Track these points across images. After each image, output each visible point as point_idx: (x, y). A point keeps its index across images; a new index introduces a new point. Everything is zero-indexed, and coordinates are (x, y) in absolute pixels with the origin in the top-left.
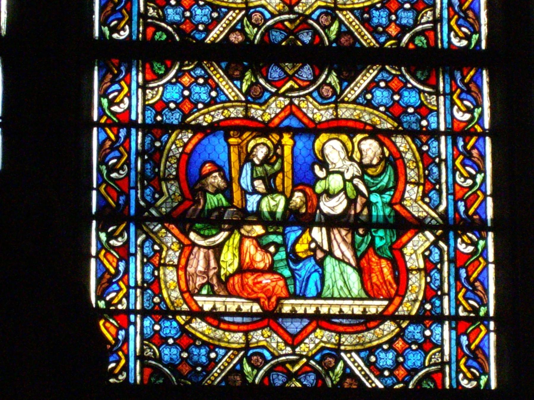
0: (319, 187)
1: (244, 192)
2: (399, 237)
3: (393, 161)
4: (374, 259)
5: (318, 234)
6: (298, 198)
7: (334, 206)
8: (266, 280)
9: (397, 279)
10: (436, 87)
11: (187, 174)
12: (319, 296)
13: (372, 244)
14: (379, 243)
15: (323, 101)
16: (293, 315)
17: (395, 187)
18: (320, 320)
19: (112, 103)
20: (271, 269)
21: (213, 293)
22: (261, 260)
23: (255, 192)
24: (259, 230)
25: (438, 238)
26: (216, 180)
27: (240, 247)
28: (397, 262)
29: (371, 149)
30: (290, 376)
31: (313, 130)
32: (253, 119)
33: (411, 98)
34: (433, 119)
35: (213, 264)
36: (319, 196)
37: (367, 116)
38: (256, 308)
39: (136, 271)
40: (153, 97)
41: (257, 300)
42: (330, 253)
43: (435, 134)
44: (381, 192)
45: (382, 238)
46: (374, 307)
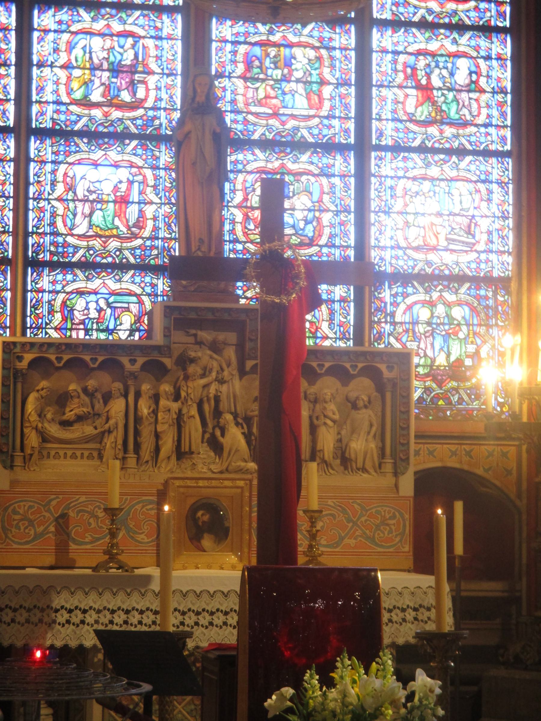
0: (293, 67)
1: (267, 68)
2: (322, 86)
4: (312, 95)
5: (293, 85)
6: (286, 71)
7: (298, 74)
8: (274, 101)
9: (320, 102)
10: (335, 31)
11: (247, 61)
12: (292, 108)
13: (311, 89)
14: (314, 89)
15: (295, 34)
16: (283, 115)
17: (320, 68)
18: (293, 117)
19: (220, 32)
20: (276, 97)
21: (255, 105)
22: (272, 93)
23: (271, 68)
24: (272, 82)
25: (335, 88)
26: (257, 63)
27: (265, 89)
28: (320, 96)
29: (312, 54)
30: (282, 137)
31: (291, 45)
32: (270, 41)
33: (326, 35)
34: (333, 42)
35: (255, 94)
36: (293, 70)
37: (310, 40)
38: (270, 111)
40: (235, 31)
41: (271, 108)
42: (296, 92)
43: (334, 48)
44: (316, 69)
45: (315, 87)
46: (312, 112)
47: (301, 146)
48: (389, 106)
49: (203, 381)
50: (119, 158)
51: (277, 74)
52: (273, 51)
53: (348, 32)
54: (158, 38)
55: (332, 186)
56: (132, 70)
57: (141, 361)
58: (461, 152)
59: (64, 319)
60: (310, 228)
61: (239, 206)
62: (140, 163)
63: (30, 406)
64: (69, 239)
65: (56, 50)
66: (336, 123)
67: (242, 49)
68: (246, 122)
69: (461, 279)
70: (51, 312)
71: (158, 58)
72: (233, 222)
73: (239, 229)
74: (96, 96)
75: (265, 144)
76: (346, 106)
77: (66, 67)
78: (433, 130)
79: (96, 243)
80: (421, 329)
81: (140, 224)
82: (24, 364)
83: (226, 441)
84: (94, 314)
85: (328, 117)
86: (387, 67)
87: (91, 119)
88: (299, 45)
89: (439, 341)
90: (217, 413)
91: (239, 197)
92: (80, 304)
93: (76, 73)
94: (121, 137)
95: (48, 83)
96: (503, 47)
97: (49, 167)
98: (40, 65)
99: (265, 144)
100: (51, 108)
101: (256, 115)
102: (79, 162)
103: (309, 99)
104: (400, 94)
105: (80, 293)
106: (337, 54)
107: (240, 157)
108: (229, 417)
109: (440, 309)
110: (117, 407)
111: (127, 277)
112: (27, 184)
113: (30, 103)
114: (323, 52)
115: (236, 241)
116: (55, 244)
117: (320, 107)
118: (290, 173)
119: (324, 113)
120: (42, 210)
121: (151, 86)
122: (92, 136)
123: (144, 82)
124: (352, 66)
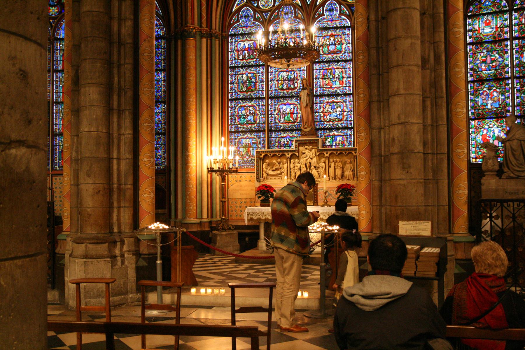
3: (342, 71)
5: (335, 79)
7: (337, 76)
18: (336, 87)
28: (343, 81)
29: (340, 70)
31: (335, 69)
39: (318, 84)
47: (338, 95)
49: (306, 158)
50: (291, 102)
51: (331, 76)
52: (330, 71)
53: (350, 64)
54: (300, 71)
55: (347, 105)
56: (294, 80)
57: (290, 154)
59: (279, 144)
60: (341, 116)
61: (322, 112)
62: (296, 103)
63: (264, 167)
64: (280, 124)
65: (275, 77)
66: (347, 88)
67: (322, 71)
68: (323, 90)
70: (275, 143)
71: (300, 76)
72: (321, 116)
73: (322, 118)
74: (285, 87)
76: (350, 83)
77: (278, 81)
79: (286, 125)
81: (297, 119)
82: (262, 156)
84: (286, 142)
85: (345, 87)
87: (284, 93)
88: (337, 68)
90: (310, 166)
91: (322, 110)
92: (282, 140)
93: (280, 82)
94: (292, 97)
95: (273, 84)
97: (274, 106)
98: (271, 81)
99: (328, 95)
100: (274, 91)
101: (326, 88)
102: (281, 104)
103: (339, 82)
105: (282, 137)
106: (347, 69)
107: (322, 99)
110: (286, 165)
111: (294, 133)
112: (268, 111)
113: (268, 91)
114: (343, 70)
115: (321, 121)
116: (276, 126)
117: (343, 84)
118: (335, 102)
119: (344, 86)
120: (272, 117)
121: (299, 83)
122: (284, 97)
123: (296, 82)
124: (351, 72)
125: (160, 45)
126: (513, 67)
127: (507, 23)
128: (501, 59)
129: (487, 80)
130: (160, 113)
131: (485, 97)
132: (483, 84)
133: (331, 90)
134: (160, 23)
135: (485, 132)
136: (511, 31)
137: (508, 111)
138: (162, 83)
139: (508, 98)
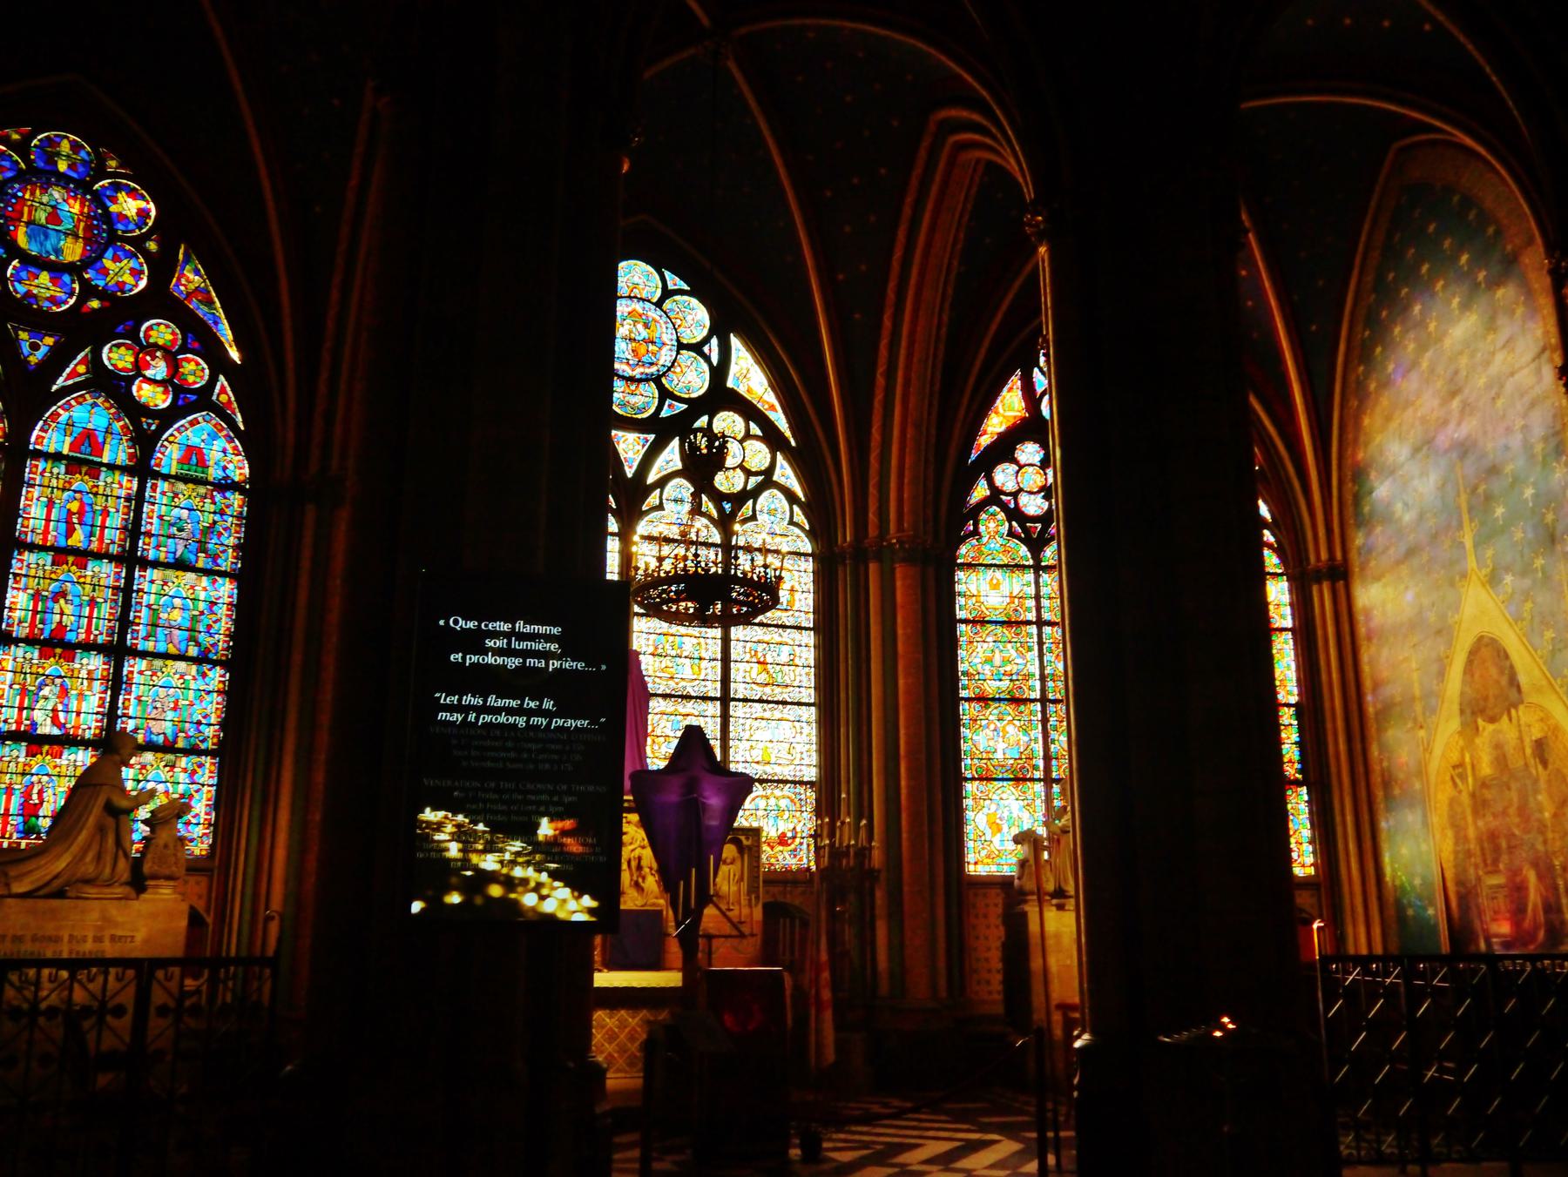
5: (683, 660)
29: (695, 641)
47: (688, 697)
48: (742, 674)
58: (784, 703)
67: (653, 637)
69: (785, 782)
75: (665, 696)
78: (768, 690)
80: (760, 813)
83: (645, 885)
86: (741, 650)
89: (771, 821)
90: (639, 868)
96: (809, 638)
99: (665, 696)
104: (748, 666)
108: (647, 870)
109: (772, 801)
125: (228, 506)
126: (1043, 678)
127: (1032, 590)
128: (1020, 661)
129: (993, 699)
130: (208, 693)
131: (991, 734)
132: (987, 706)
133: (672, 684)
134: (235, 448)
135: (993, 807)
136: (1039, 608)
137: (1035, 768)
138: (222, 610)
139: (1036, 741)
